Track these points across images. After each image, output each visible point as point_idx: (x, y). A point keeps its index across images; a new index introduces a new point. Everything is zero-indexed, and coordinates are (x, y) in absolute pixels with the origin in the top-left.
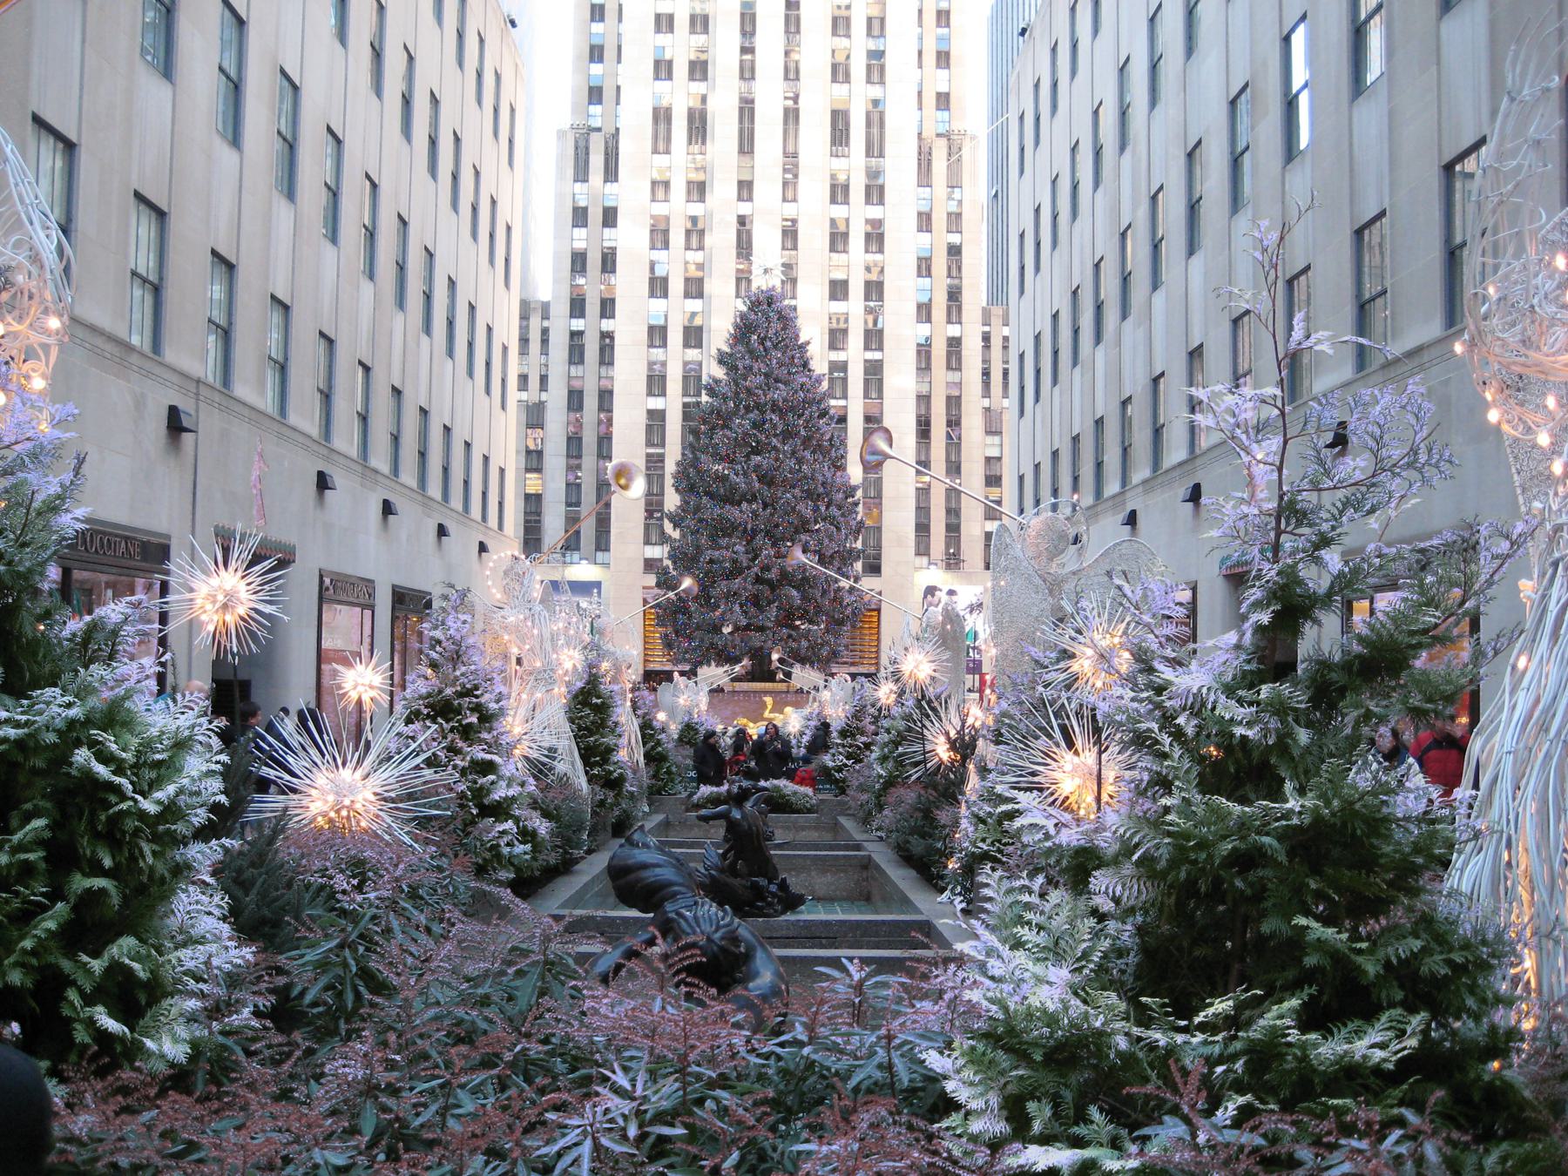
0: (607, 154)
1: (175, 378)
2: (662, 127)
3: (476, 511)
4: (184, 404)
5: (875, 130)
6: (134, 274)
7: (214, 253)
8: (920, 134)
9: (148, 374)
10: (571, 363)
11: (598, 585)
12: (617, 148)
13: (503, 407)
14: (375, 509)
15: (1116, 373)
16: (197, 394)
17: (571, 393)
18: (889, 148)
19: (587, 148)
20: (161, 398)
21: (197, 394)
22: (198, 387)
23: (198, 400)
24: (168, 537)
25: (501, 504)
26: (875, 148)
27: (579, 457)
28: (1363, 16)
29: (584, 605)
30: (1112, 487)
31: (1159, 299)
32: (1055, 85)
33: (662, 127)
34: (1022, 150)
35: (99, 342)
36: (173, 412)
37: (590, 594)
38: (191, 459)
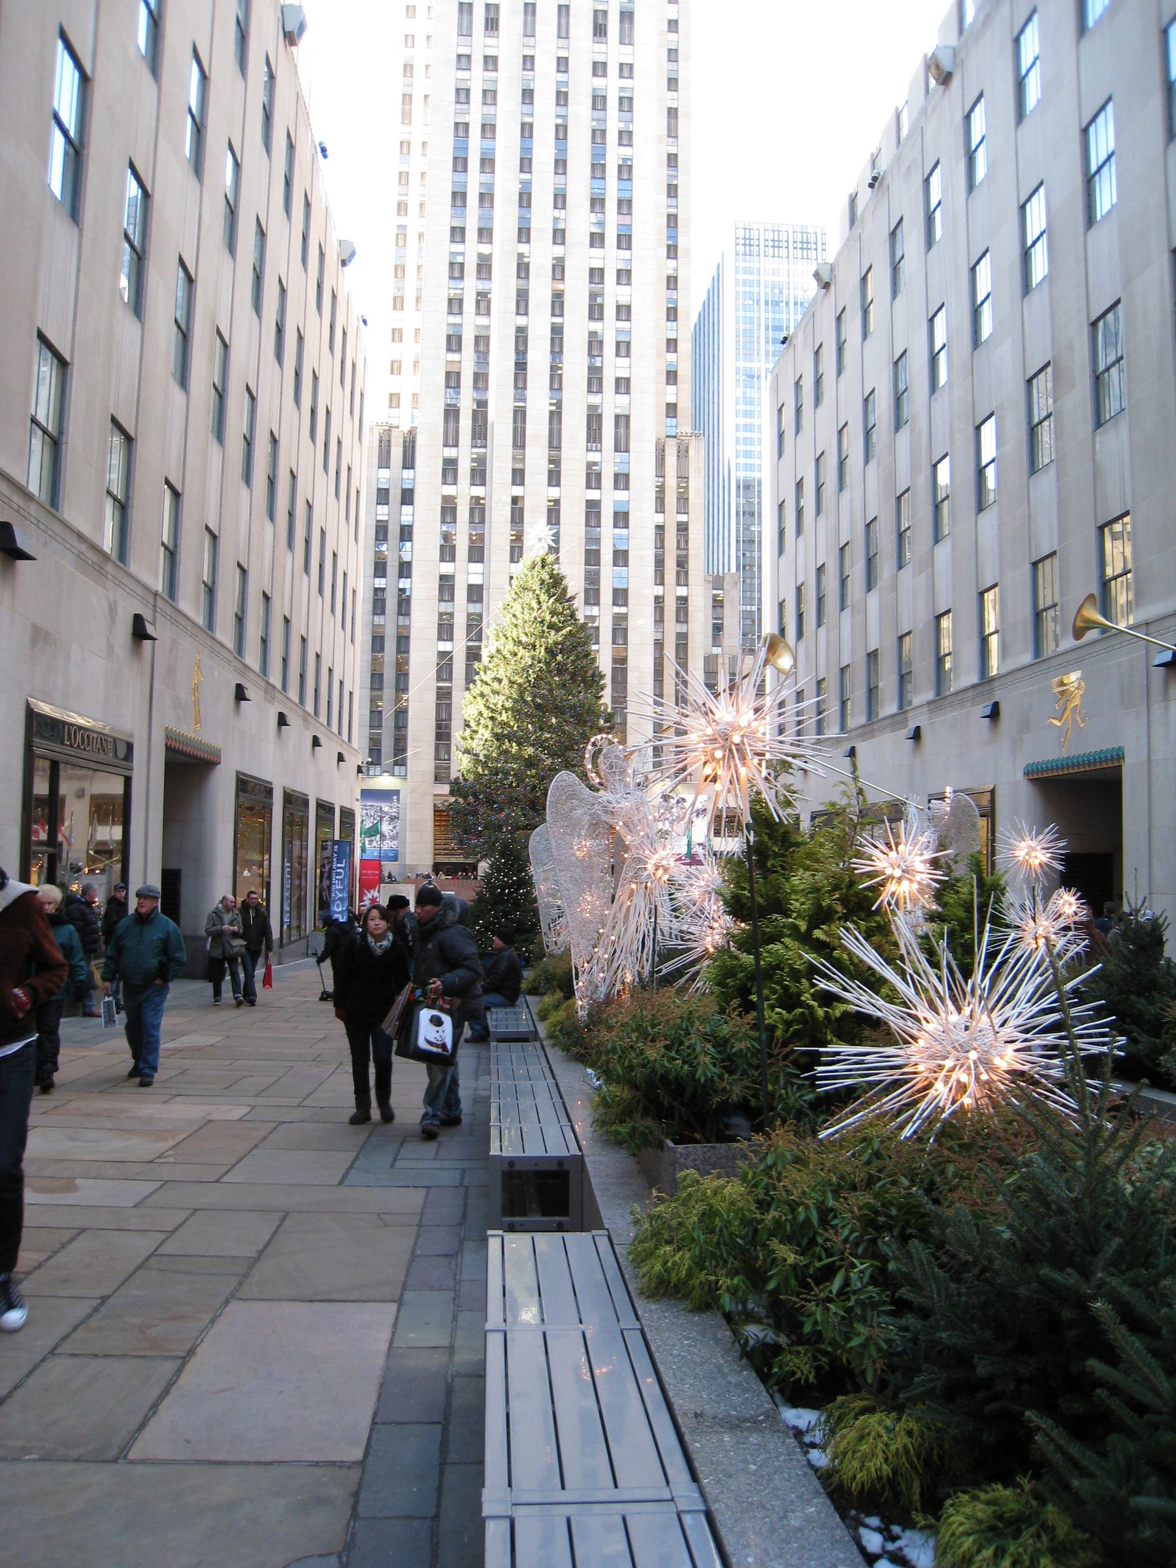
0: (405, 447)
1: (139, 590)
2: (451, 425)
3: (335, 729)
4: (147, 615)
5: (622, 431)
9: (119, 584)
10: (375, 613)
11: (397, 793)
12: (414, 442)
13: (352, 641)
14: (273, 720)
15: (892, 611)
16: (155, 606)
17: (374, 638)
18: (633, 446)
20: (129, 607)
21: (155, 606)
22: (155, 599)
23: (155, 611)
24: (132, 736)
25: (350, 722)
26: (622, 445)
27: (381, 689)
29: (386, 809)
30: (889, 708)
31: (943, 552)
32: (818, 382)
33: (451, 425)
34: (781, 436)
35: (83, 547)
36: (138, 620)
37: (391, 800)
38: (149, 663)
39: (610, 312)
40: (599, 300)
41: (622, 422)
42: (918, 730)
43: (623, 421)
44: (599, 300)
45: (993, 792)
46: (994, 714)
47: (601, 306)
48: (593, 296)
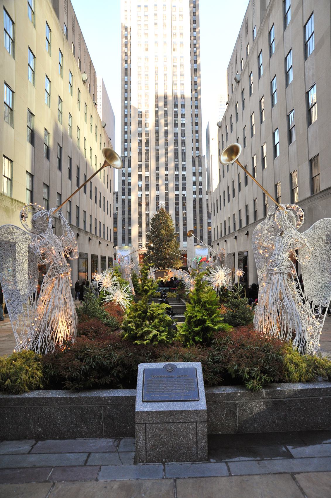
3: (106, 238)
6: (44, 198)
7: (57, 193)
8: (193, 156)
14: (88, 239)
19: (125, 161)
25: (110, 236)
26: (184, 160)
27: (125, 224)
28: (276, 144)
33: (140, 156)
39: (179, 125)
40: (177, 122)
41: (184, 154)
42: (236, 236)
43: (184, 153)
44: (177, 122)
45: (248, 252)
46: (247, 234)
47: (177, 124)
48: (175, 121)
